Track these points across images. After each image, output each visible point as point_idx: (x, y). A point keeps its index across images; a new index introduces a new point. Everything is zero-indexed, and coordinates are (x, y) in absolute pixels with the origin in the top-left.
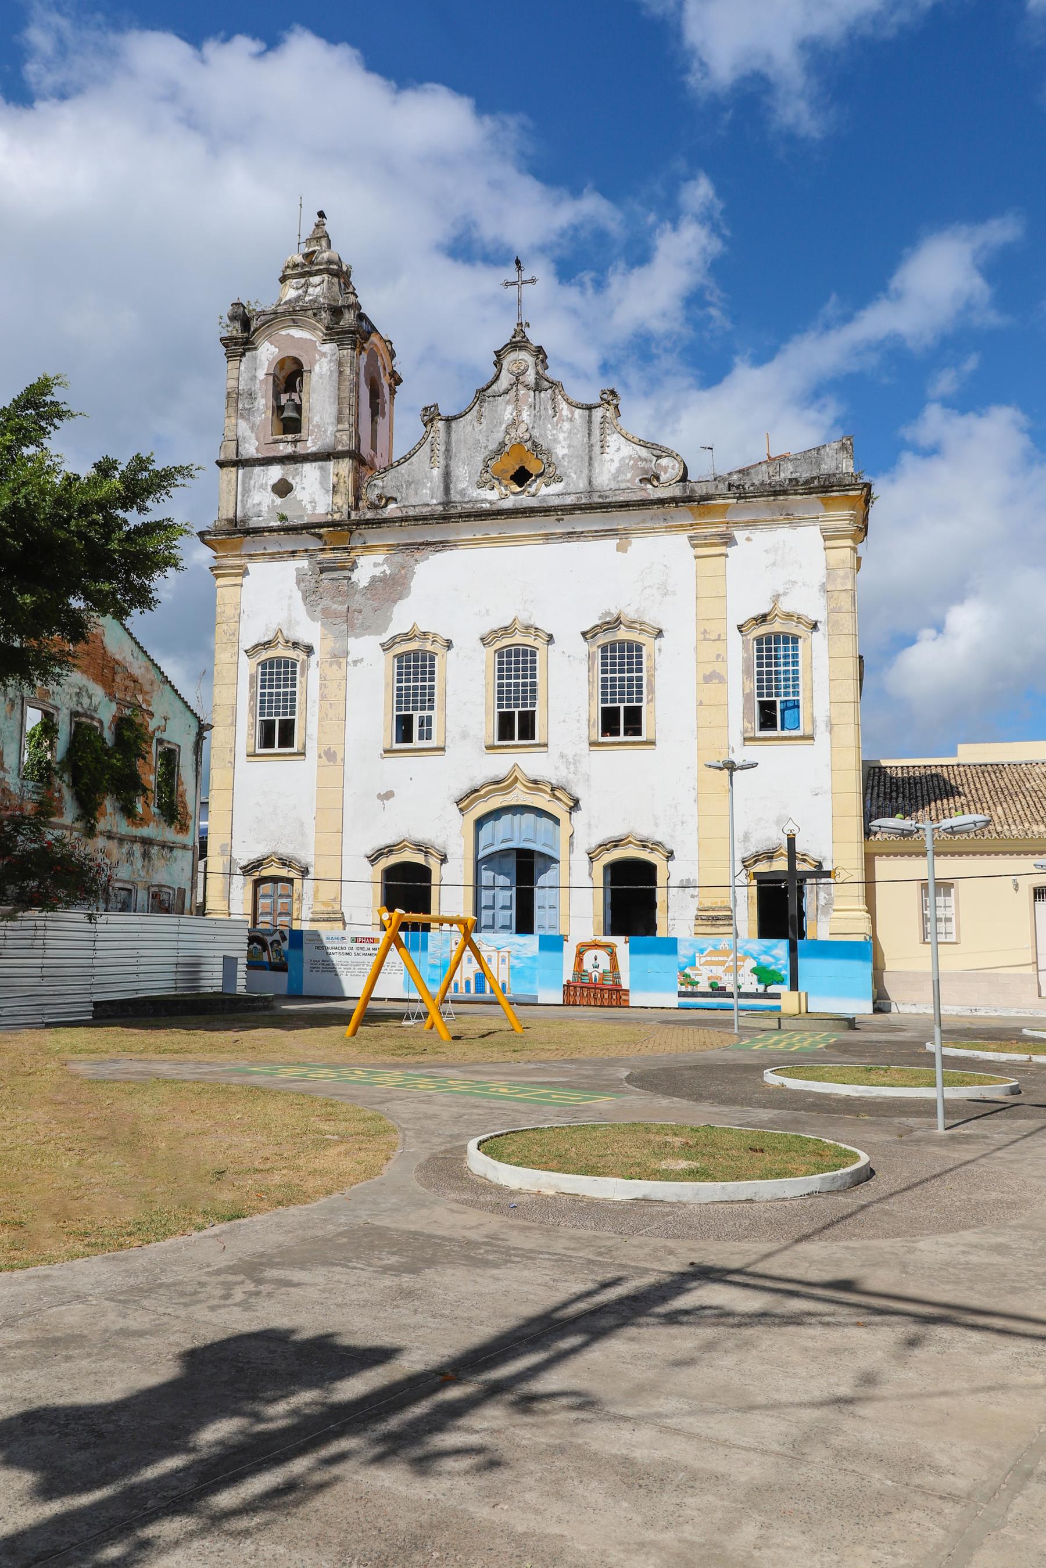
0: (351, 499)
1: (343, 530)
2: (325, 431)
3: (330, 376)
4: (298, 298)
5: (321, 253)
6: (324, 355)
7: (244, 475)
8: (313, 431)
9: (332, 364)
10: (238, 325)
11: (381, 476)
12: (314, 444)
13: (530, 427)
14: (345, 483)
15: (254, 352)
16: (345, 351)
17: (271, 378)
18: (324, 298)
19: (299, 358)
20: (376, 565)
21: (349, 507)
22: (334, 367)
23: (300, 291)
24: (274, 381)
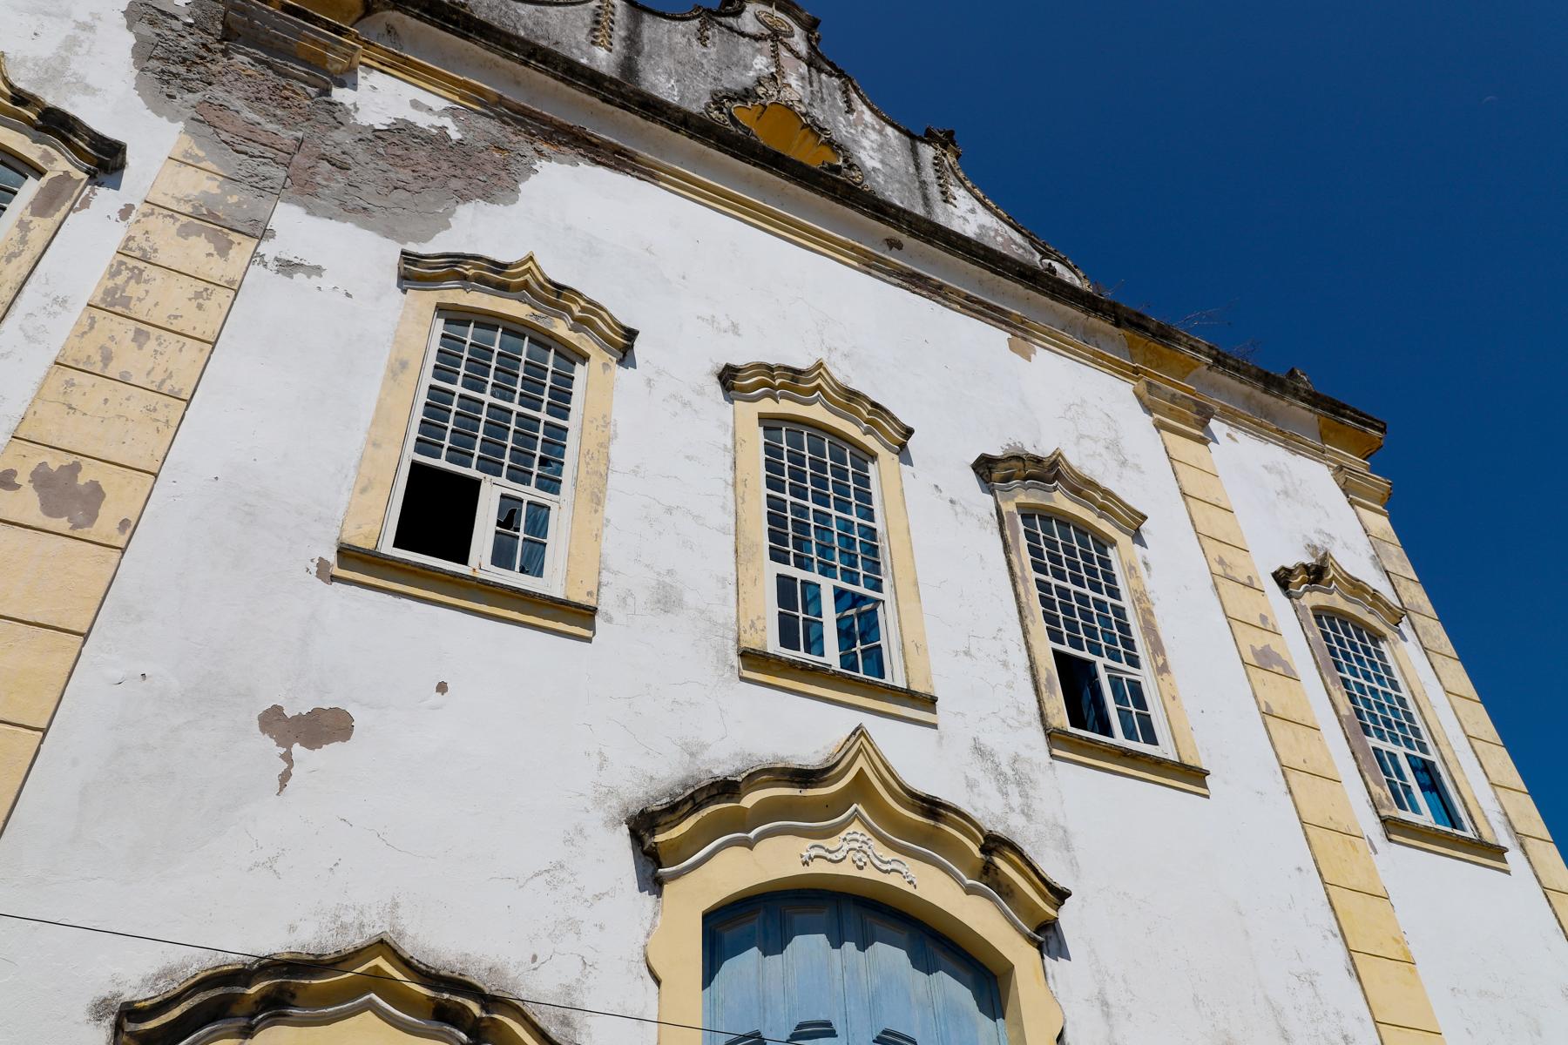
13: (806, 101)
20: (416, 104)
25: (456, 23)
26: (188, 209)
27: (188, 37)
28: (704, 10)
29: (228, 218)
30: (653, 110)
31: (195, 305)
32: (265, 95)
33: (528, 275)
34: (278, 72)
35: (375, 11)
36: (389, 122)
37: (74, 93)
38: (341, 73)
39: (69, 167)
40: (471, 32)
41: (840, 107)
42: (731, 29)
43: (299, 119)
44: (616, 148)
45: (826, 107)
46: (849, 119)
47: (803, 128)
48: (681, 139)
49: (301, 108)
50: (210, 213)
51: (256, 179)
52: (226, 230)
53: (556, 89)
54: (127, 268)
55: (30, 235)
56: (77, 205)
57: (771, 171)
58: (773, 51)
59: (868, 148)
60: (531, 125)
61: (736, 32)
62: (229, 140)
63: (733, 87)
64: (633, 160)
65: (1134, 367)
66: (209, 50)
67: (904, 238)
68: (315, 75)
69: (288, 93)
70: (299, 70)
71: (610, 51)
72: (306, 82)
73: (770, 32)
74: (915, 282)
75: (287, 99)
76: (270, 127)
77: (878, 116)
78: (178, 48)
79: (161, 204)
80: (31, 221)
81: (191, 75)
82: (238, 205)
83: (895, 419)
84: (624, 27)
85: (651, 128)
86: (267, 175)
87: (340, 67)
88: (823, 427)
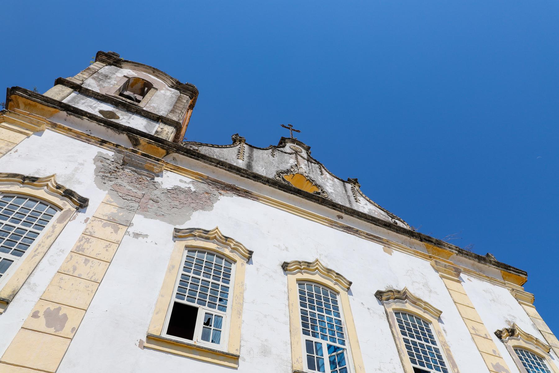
15: (119, 68)
20: (181, 181)
24: (127, 82)
25: (195, 155)
26: (106, 218)
27: (112, 165)
28: (273, 146)
29: (119, 220)
30: (257, 178)
31: (105, 250)
32: (134, 181)
33: (216, 234)
34: (138, 174)
35: (170, 153)
36: (172, 187)
37: (75, 184)
38: (158, 173)
39: (71, 207)
40: (199, 158)
41: (319, 173)
42: (282, 151)
43: (144, 187)
44: (246, 191)
45: (314, 174)
46: (322, 177)
47: (307, 181)
48: (267, 187)
49: (145, 184)
50: (113, 219)
51: (129, 207)
52: (118, 224)
53: (226, 173)
54: (85, 239)
55: (56, 230)
56: (71, 219)
57: (297, 195)
58: (296, 157)
59: (329, 186)
60: (218, 185)
61: (284, 152)
62: (121, 195)
63: (283, 169)
64: (251, 194)
65: (429, 256)
66: (118, 168)
67: (343, 215)
68: (150, 174)
69: (141, 180)
70: (145, 173)
71: (243, 160)
72: (147, 176)
73: (294, 152)
74: (348, 229)
75: (141, 182)
76: (135, 191)
77: (331, 175)
78: (108, 169)
79: (98, 217)
80: (56, 225)
81: (112, 176)
82: (122, 216)
83: (345, 279)
84: (247, 153)
85: (257, 184)
86: (132, 206)
87: (158, 171)
88: (319, 283)
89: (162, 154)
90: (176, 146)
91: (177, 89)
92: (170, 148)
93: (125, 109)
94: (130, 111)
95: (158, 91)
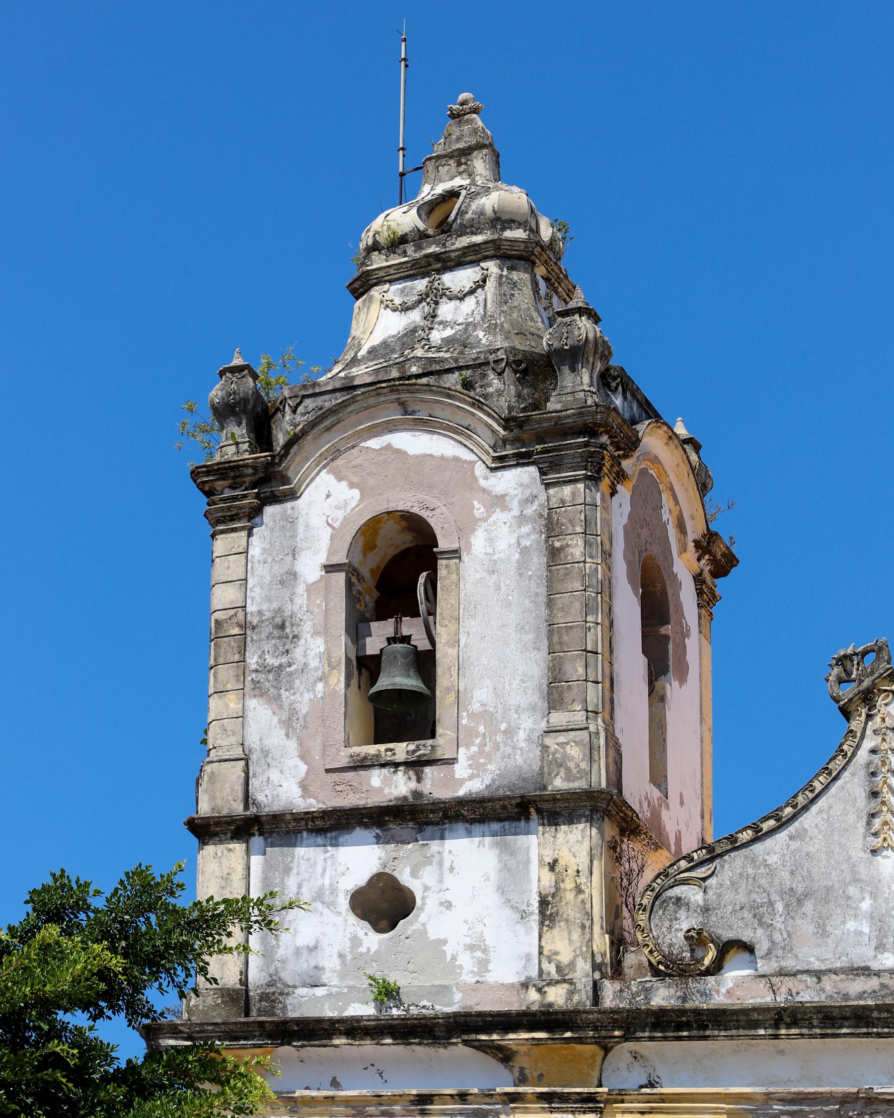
0: (602, 943)
1: (580, 1041)
2: (509, 733)
3: (522, 565)
4: (410, 337)
5: (473, 196)
6: (499, 501)
7: (268, 868)
8: (472, 733)
9: (526, 529)
10: (240, 431)
11: (701, 872)
12: (477, 768)
14: (579, 890)
15: (288, 505)
16: (567, 490)
17: (340, 579)
18: (491, 329)
19: (424, 514)
21: (596, 967)
22: (531, 535)
23: (415, 316)
24: (349, 585)
25: (687, 1026)
35: (612, 1048)
40: (705, 1028)
89: (593, 1057)
90: (616, 1016)
91: (522, 460)
92: (605, 1038)
93: (411, 824)
94: (427, 824)
95: (464, 556)
